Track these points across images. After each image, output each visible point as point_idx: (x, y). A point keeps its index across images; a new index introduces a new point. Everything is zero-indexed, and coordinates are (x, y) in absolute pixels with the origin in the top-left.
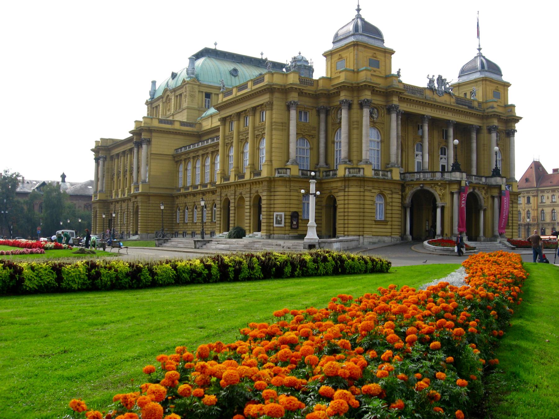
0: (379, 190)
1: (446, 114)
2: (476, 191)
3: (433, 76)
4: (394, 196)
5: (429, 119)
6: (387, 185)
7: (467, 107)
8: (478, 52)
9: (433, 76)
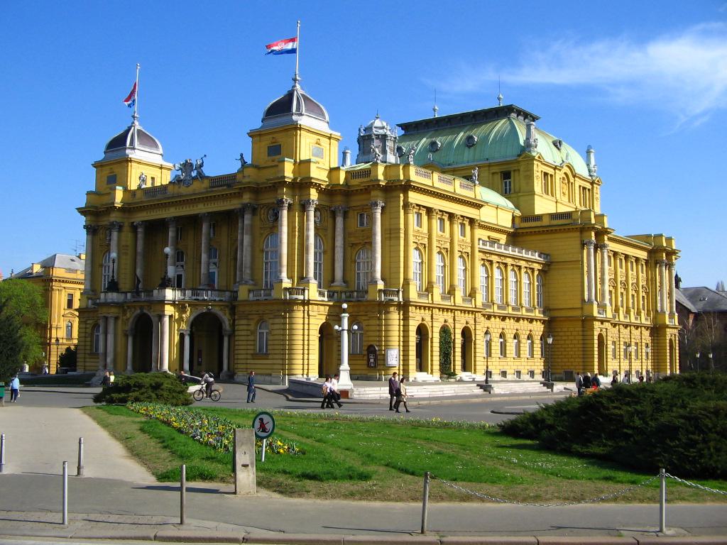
1: (195, 208)
2: (145, 311)
7: (225, 187)
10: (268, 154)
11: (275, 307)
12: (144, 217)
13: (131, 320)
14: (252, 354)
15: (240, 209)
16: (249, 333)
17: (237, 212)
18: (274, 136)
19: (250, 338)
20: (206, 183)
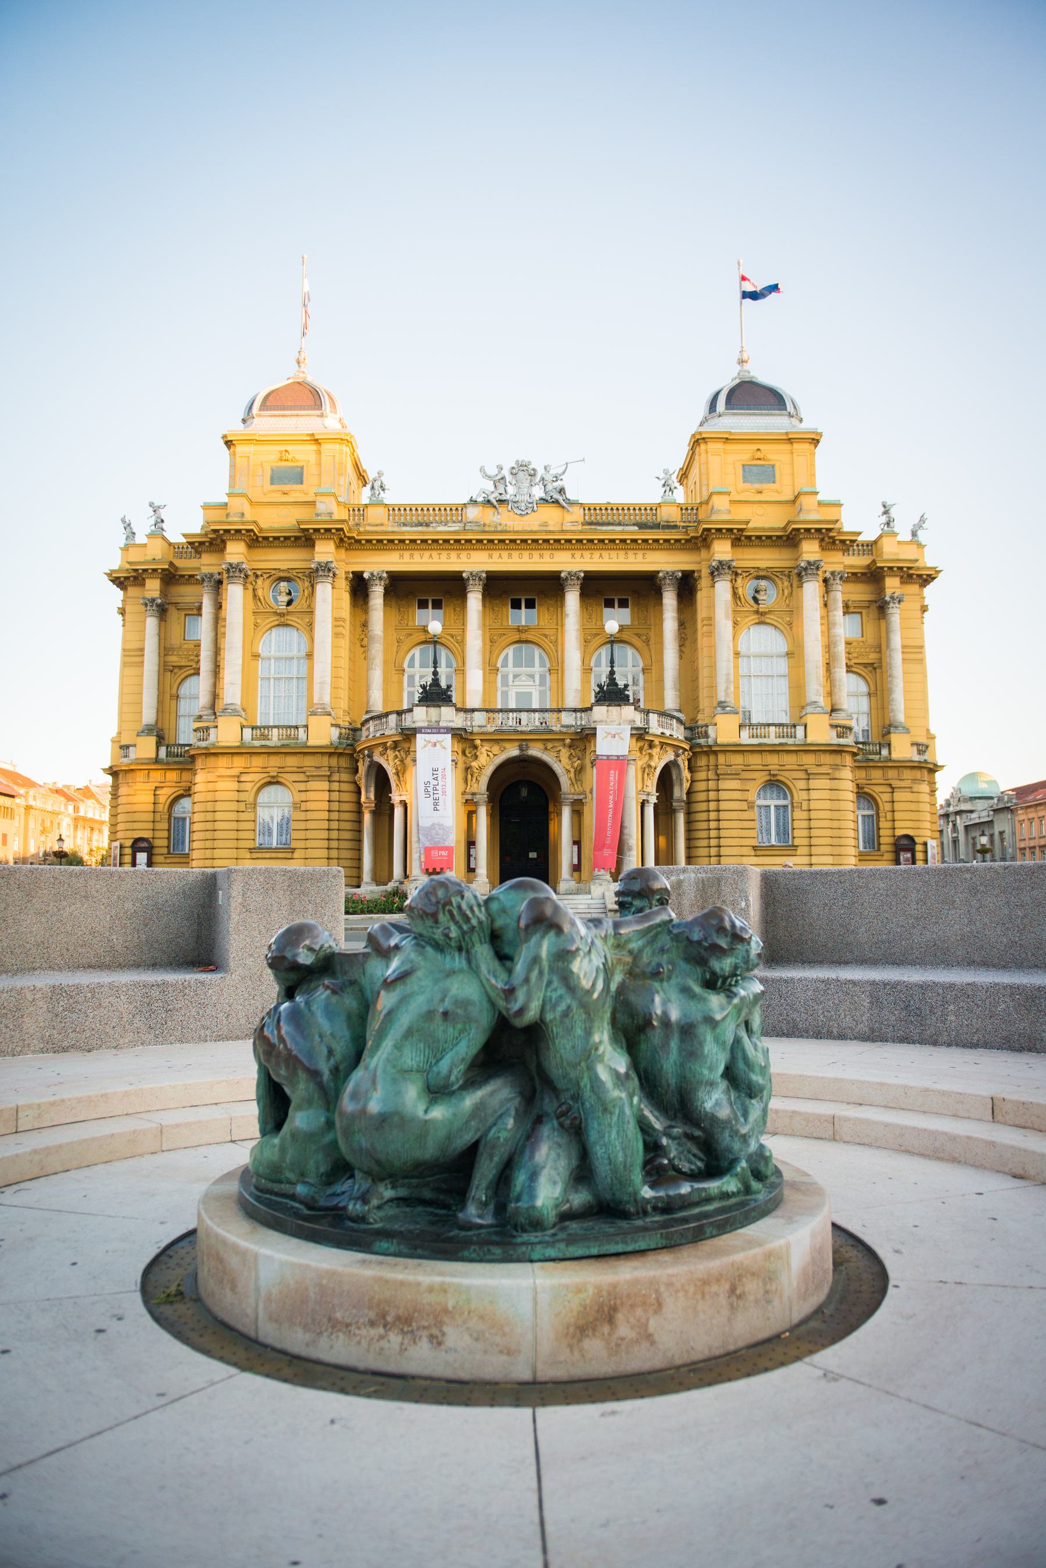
0: (267, 775)
2: (535, 751)
3: (500, 468)
4: (313, 785)
5: (480, 579)
6: (292, 761)
8: (738, 368)
9: (500, 468)
10: (744, 477)
11: (808, 760)
12: (392, 563)
13: (489, 771)
14: (753, 847)
15: (673, 573)
16: (744, 806)
17: (665, 578)
18: (762, 447)
19: (746, 815)
20: (577, 514)
